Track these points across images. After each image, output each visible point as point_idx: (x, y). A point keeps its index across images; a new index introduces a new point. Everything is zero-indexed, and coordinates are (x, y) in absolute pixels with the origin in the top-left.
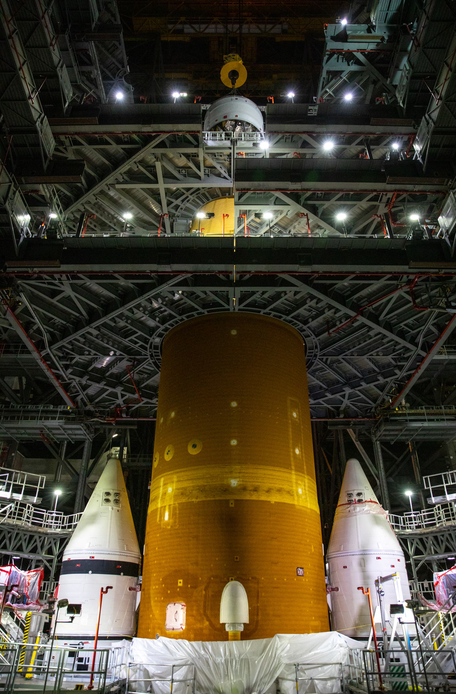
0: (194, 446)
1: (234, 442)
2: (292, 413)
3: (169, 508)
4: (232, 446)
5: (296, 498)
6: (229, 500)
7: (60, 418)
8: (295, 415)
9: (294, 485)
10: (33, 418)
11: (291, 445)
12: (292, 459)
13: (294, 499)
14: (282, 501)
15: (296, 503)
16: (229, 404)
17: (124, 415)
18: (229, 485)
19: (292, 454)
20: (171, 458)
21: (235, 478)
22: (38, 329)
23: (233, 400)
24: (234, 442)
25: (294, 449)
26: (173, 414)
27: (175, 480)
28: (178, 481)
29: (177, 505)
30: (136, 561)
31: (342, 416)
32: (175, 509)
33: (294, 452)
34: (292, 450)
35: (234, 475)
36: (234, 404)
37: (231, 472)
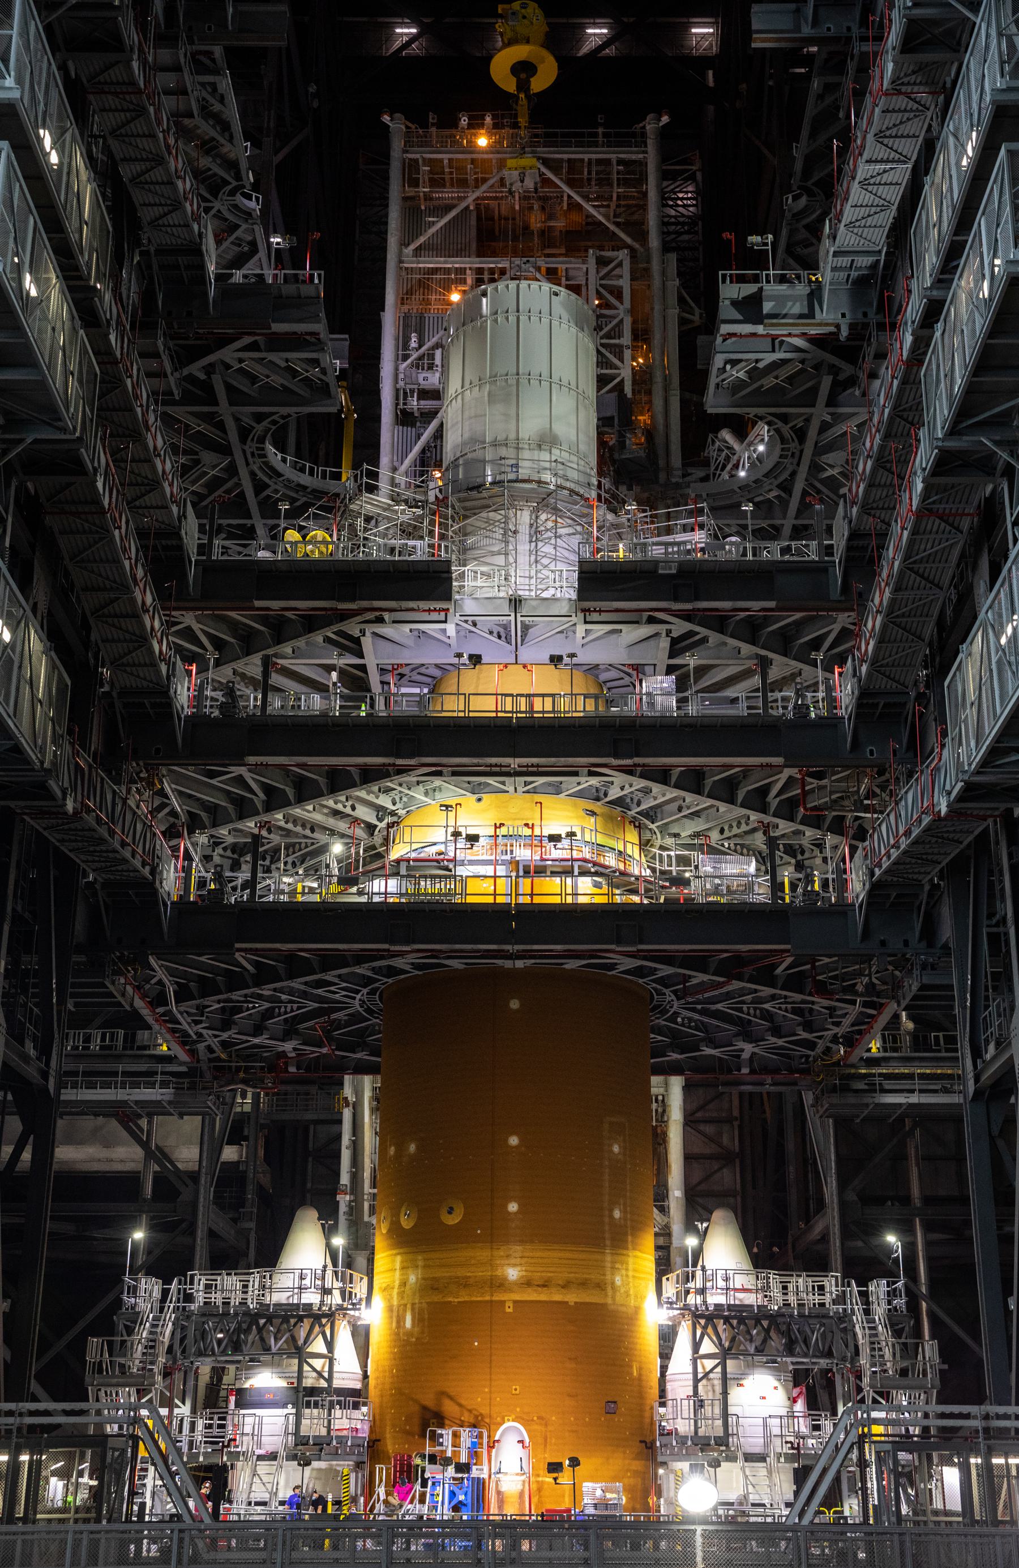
0: (450, 1211)
1: (513, 1207)
2: (611, 1145)
3: (413, 1310)
4: (509, 1213)
5: (610, 1292)
6: (504, 1302)
7: (164, 1085)
8: (616, 1149)
9: (608, 1273)
10: (106, 1086)
11: (606, 1205)
12: (607, 1228)
13: (606, 1295)
14: (588, 1300)
15: (609, 1301)
16: (506, 1140)
17: (292, 1069)
18: (505, 1279)
19: (606, 1220)
20: (412, 1224)
21: (514, 1265)
22: (160, 980)
23: (512, 1134)
24: (513, 1207)
25: (611, 1211)
26: (412, 1148)
27: (420, 1263)
28: (425, 1267)
29: (424, 1305)
30: (358, 1386)
31: (745, 1070)
32: (421, 1311)
33: (611, 1216)
34: (607, 1213)
35: (513, 1261)
36: (514, 1141)
37: (508, 1256)
